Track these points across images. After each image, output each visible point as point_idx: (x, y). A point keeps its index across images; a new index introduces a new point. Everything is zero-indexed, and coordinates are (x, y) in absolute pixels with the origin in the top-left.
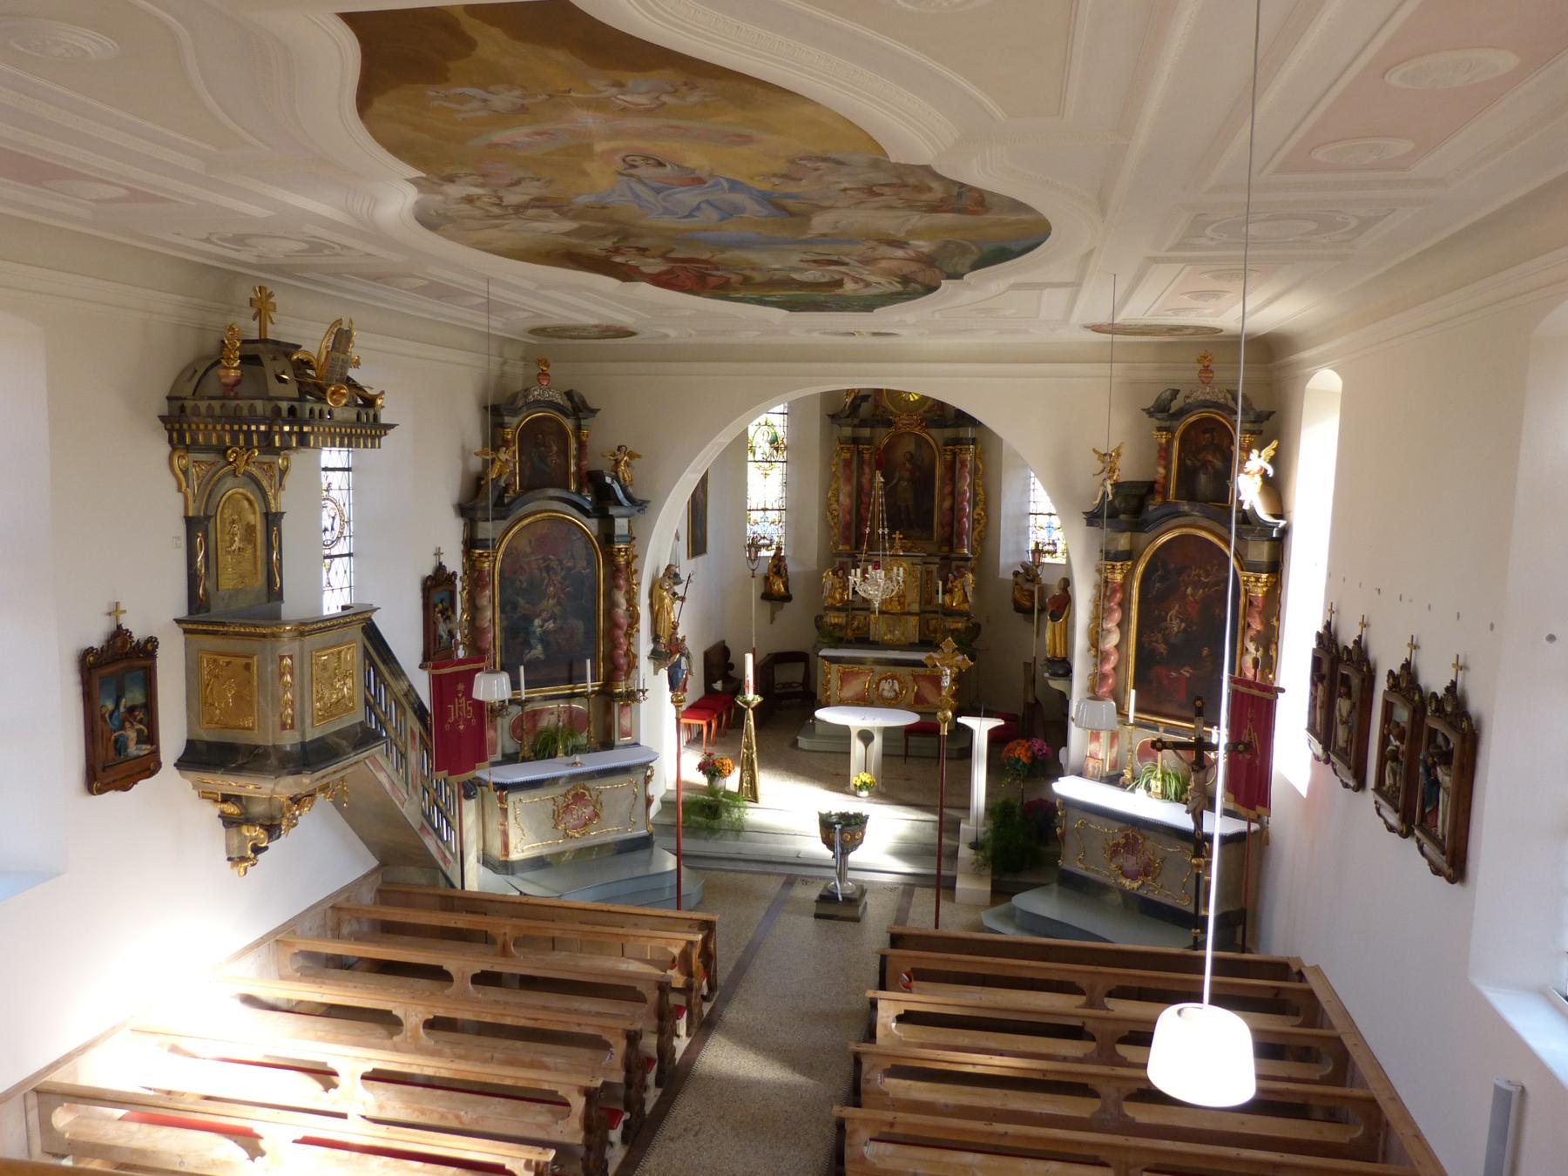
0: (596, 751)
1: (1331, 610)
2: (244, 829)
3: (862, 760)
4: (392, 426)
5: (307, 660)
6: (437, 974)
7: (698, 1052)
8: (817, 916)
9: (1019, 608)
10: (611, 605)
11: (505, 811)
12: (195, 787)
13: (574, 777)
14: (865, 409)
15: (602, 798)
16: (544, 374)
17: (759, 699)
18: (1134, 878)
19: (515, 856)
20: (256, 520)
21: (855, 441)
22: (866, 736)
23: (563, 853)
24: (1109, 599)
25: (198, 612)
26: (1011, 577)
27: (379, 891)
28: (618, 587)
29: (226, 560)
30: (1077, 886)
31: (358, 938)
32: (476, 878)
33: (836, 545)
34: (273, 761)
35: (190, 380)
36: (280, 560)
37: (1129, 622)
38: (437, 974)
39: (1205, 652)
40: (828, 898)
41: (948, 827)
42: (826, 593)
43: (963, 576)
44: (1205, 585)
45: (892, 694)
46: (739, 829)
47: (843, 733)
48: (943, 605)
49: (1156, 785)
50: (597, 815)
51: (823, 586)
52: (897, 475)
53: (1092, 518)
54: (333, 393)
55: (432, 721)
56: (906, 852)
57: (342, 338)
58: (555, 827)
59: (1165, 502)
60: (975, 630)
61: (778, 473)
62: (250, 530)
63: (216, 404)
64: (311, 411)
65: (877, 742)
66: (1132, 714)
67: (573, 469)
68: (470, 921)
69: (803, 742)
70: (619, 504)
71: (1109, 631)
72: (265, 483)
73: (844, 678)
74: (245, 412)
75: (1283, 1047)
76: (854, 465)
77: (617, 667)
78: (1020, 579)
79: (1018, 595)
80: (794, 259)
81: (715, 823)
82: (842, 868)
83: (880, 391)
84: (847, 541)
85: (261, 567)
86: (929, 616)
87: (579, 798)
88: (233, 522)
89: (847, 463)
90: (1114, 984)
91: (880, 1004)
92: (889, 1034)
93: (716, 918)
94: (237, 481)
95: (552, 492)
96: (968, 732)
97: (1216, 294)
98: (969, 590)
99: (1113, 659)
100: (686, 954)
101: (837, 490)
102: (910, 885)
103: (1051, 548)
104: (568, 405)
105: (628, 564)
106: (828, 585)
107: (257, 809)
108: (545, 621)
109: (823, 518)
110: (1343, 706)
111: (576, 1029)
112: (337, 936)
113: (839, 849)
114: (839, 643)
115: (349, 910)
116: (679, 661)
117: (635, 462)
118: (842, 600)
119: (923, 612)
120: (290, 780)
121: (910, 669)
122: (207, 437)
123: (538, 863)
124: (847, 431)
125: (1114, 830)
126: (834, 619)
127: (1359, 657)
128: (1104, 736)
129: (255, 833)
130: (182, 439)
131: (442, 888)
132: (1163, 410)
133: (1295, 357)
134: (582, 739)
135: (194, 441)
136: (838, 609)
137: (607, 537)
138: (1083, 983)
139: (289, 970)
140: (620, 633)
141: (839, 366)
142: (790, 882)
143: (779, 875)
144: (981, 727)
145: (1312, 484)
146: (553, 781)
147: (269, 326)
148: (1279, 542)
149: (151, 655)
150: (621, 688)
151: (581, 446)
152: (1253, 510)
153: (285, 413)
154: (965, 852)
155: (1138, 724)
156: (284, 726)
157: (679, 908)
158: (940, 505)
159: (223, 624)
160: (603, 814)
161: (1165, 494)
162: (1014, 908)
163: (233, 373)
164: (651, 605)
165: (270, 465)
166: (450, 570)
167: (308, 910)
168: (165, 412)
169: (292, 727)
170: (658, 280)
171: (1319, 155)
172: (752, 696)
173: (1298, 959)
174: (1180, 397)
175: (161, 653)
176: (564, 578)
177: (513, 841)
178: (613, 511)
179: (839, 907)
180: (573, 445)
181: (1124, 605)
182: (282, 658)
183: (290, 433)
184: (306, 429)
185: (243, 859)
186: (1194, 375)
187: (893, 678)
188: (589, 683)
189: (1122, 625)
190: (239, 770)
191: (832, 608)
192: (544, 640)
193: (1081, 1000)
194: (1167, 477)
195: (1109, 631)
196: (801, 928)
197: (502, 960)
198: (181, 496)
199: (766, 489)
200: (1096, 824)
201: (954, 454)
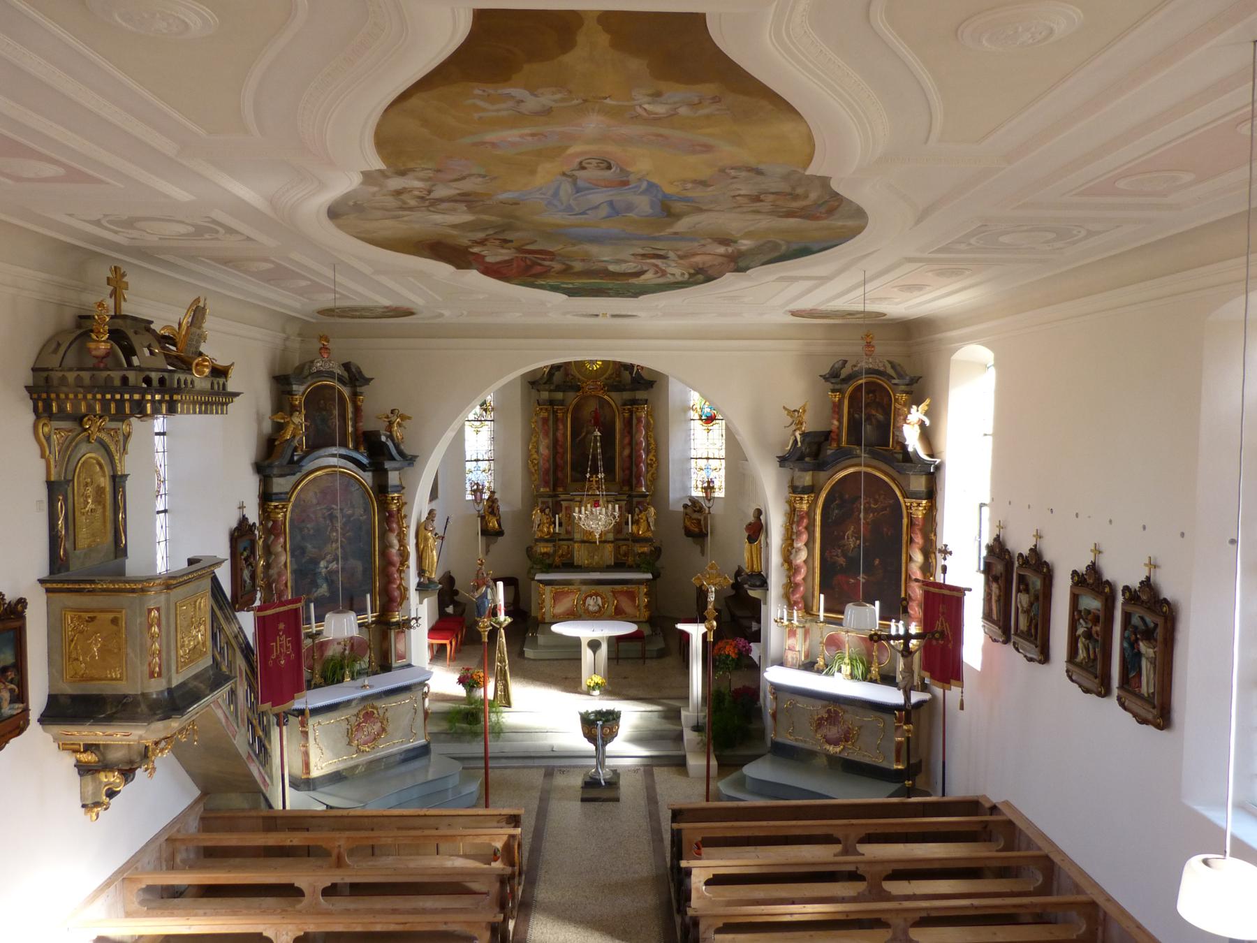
0: (375, 673)
1: (1000, 527)
2: (103, 777)
3: (592, 665)
4: (237, 394)
5: (172, 611)
6: (289, 892)
7: (526, 932)
8: (583, 800)
9: (688, 533)
10: (385, 547)
11: (305, 734)
12: (55, 740)
13: (364, 698)
14: (558, 376)
15: (388, 714)
16: (325, 348)
17: (509, 620)
18: (836, 743)
19: (315, 773)
20: (105, 482)
21: (552, 402)
22: (595, 645)
23: (356, 766)
24: (799, 524)
25: (59, 572)
27: (202, 819)
28: (391, 530)
29: (82, 520)
30: (784, 752)
31: (191, 866)
32: (295, 801)
33: (537, 488)
34: (143, 708)
35: (55, 351)
36: (125, 519)
37: (814, 542)
38: (289, 892)
39: (877, 562)
40: (591, 784)
41: (673, 715)
42: (535, 528)
43: (646, 509)
44: (874, 511)
45: (596, 608)
46: (499, 731)
47: (575, 643)
48: (632, 534)
49: (846, 669)
50: (384, 730)
51: (533, 522)
53: (783, 461)
54: (197, 365)
55: (257, 657)
56: (640, 739)
57: (198, 313)
58: (349, 744)
59: (839, 447)
60: (657, 552)
61: (486, 430)
62: (100, 491)
63: (86, 375)
64: (179, 381)
65: (604, 648)
66: (822, 614)
67: (350, 429)
68: (297, 838)
69: (529, 653)
70: (393, 459)
71: (799, 549)
72: (113, 448)
73: (557, 597)
74: (117, 382)
75: (1006, 868)
76: (551, 422)
77: (390, 600)
78: (689, 511)
79: (688, 524)
80: (626, 253)
81: (479, 728)
82: (600, 756)
83: (570, 363)
84: (546, 484)
85: (110, 526)
86: (621, 543)
87: (368, 716)
88: (87, 485)
89: (545, 421)
90: (863, 832)
91: (694, 872)
92: (701, 897)
93: (521, 812)
94: (90, 446)
95: (334, 450)
96: (685, 637)
97: (919, 288)
98: (651, 520)
99: (803, 571)
100: (508, 847)
101: (537, 442)
102: (650, 765)
104: (346, 374)
105: (399, 510)
106: (537, 522)
107: (114, 756)
108: (329, 562)
110: (1020, 600)
111: (443, 928)
112: (172, 867)
113: (600, 742)
114: (550, 568)
115: (183, 840)
116: (486, 592)
117: (406, 423)
118: (549, 533)
119: (616, 540)
120: (159, 725)
121: (609, 587)
122: (76, 406)
123: (336, 778)
124: (545, 395)
125: (819, 709)
126: (543, 548)
127: (1037, 564)
128: (800, 632)
129: (113, 778)
130: (48, 407)
131: (264, 812)
132: (836, 377)
133: (939, 336)
134: (363, 664)
135: (61, 409)
136: (547, 541)
137: (382, 489)
138: (838, 834)
139: (135, 905)
140: (394, 569)
141: (585, 342)
142: (549, 773)
143: (538, 767)
144: (696, 632)
145: (966, 434)
146: (348, 703)
147: (123, 304)
148: (933, 476)
149: (21, 617)
150: (397, 618)
151: (357, 410)
152: (916, 452)
153: (155, 383)
154: (689, 735)
155: (828, 621)
156: (152, 675)
157: (487, 807)
158: (621, 452)
159: (92, 582)
160: (390, 728)
161: (839, 441)
162: (744, 776)
163: (102, 346)
164: (417, 545)
165: (116, 430)
166: (251, 521)
167: (147, 845)
168: (30, 383)
169: (160, 675)
170: (493, 271)
171: (1121, 184)
172: (502, 617)
173: (984, 796)
174: (848, 366)
175: (29, 613)
176: (345, 524)
177: (313, 760)
178: (387, 465)
179: (600, 790)
180: (350, 409)
181: (810, 529)
182: (150, 611)
183: (160, 402)
184: (175, 397)
185: (97, 804)
186: (859, 348)
187: (597, 595)
188: (370, 615)
189: (809, 544)
190: (110, 719)
191: (541, 540)
192: (330, 579)
193: (838, 848)
194: (840, 428)
195: (799, 549)
196: (568, 812)
197: (338, 872)
198: (43, 462)
199: (479, 441)
200: (802, 703)
201: (631, 412)
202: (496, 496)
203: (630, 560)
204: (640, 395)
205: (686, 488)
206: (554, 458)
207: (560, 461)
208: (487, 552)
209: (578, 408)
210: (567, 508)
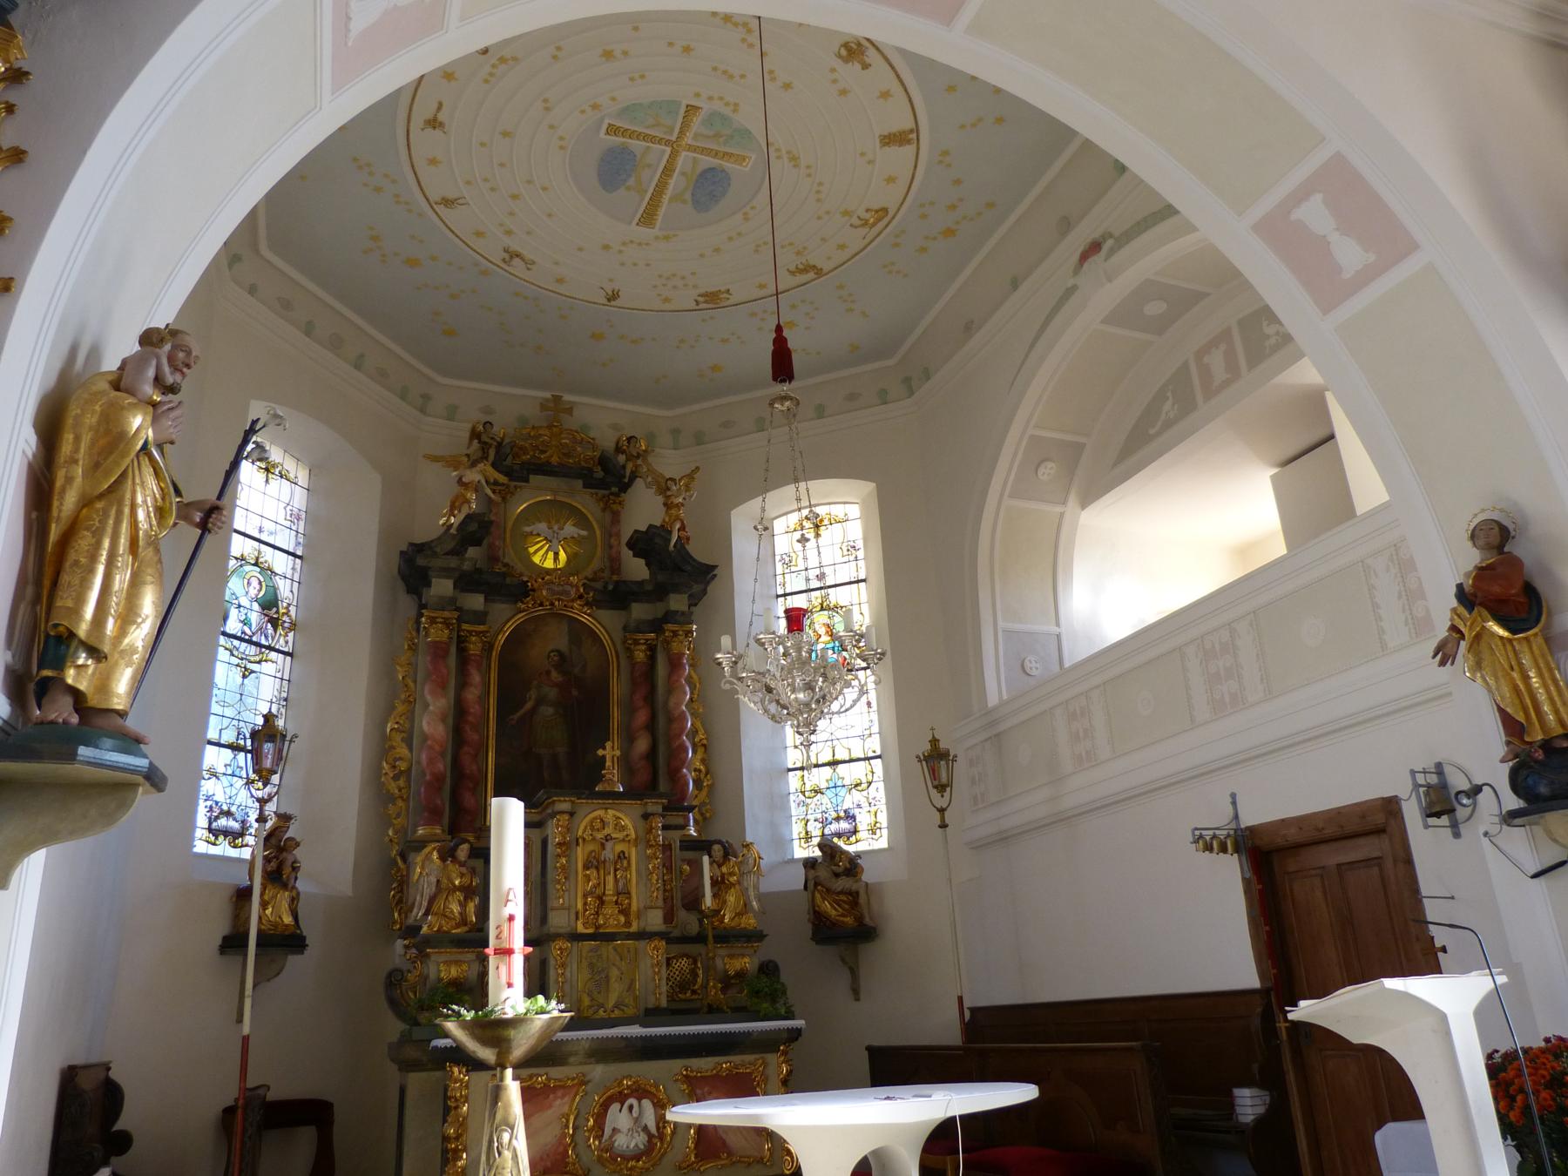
45: (640, 1140)
52: (533, 694)
76: (452, 660)
78: (823, 873)
79: (827, 907)
84: (434, 815)
89: (438, 651)
101: (410, 716)
103: (844, 825)
109: (374, 779)
118: (464, 921)
121: (676, 1065)
187: (640, 1092)
203: (714, 992)
204: (677, 602)
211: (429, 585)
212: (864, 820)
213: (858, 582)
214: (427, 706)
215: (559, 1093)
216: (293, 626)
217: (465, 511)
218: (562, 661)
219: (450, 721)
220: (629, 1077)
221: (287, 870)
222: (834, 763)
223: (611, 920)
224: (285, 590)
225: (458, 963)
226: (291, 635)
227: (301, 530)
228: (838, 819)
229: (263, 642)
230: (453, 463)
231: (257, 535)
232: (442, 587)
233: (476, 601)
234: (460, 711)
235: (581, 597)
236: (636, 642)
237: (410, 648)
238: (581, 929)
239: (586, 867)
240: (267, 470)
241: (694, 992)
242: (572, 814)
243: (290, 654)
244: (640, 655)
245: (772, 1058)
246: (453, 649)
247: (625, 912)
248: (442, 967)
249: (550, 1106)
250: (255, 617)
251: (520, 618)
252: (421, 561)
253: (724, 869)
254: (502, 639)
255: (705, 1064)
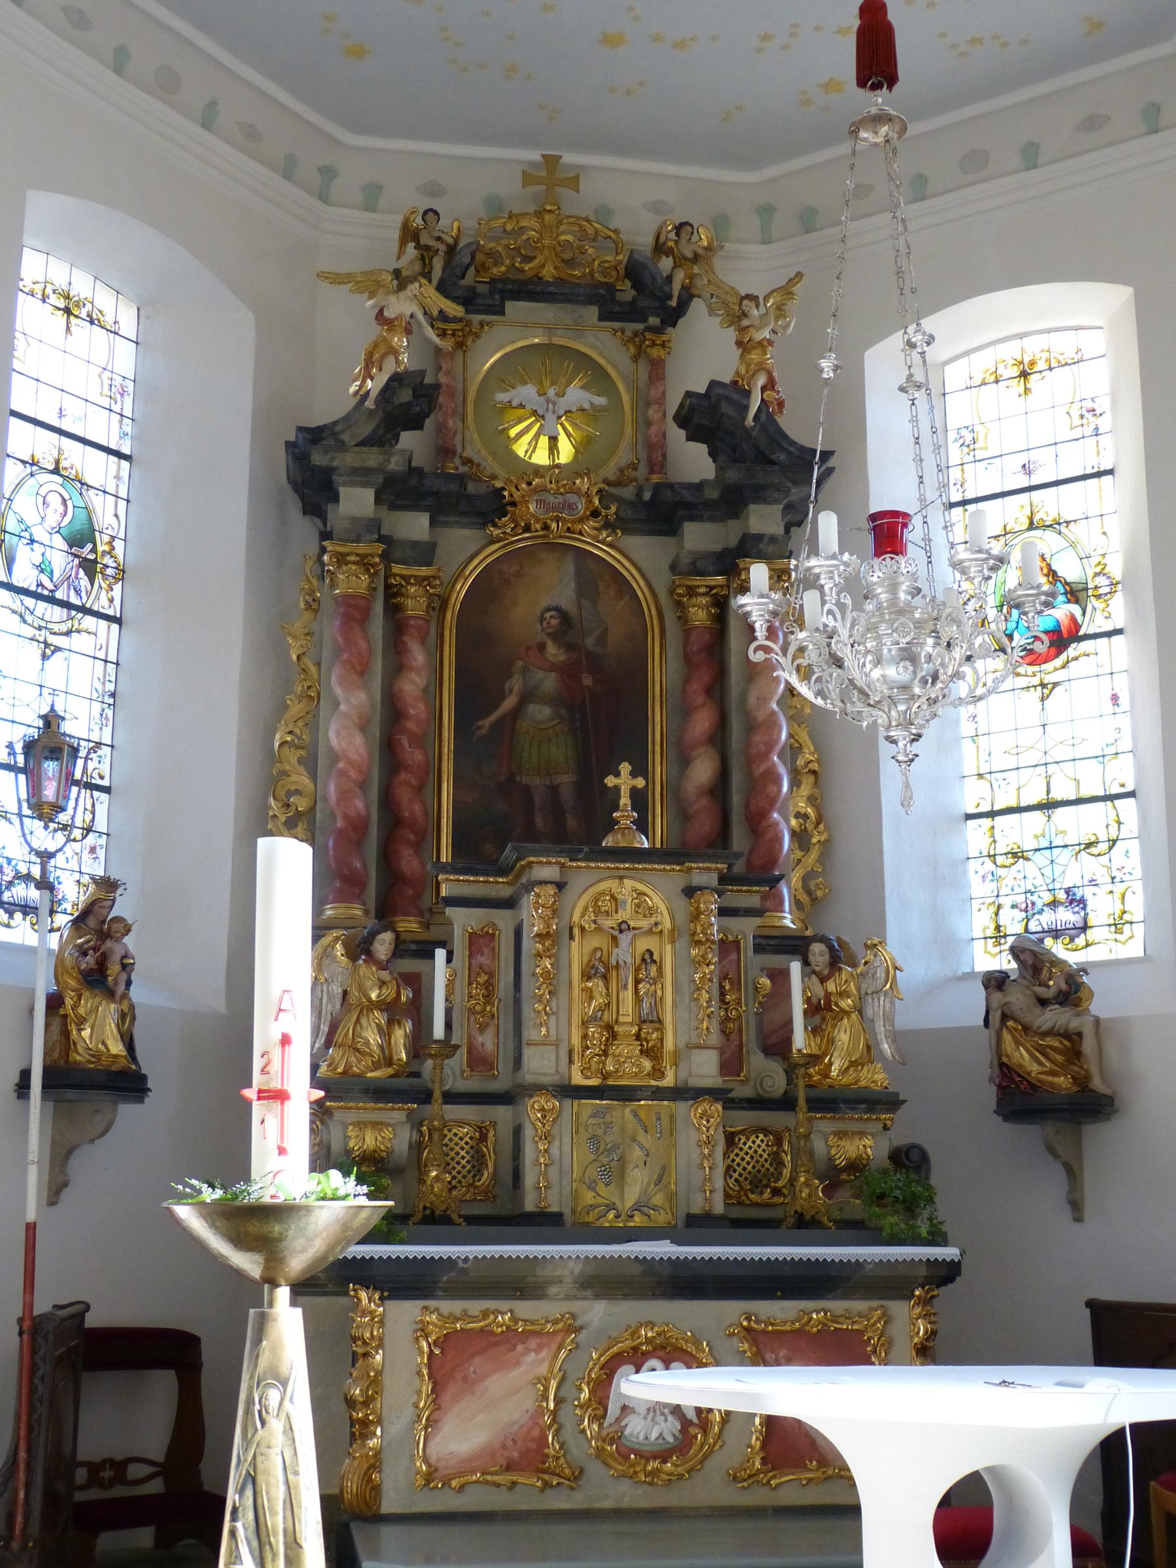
9: (1017, 1098)
26: (971, 1007)
52: (516, 684)
76: (377, 626)
78: (1017, 998)
79: (1023, 1057)
89: (354, 612)
101: (312, 721)
103: (1066, 916)
121: (733, 1310)
136: (380, 1093)
172: (283, 1159)
201: (721, 605)
202: (123, 907)
203: (809, 1193)
204: (764, 519)
205: (948, 943)
206: (387, 800)
207: (411, 807)
208: (56, 1189)
209: (489, 589)
210: (480, 941)
211: (335, 498)
212: (1100, 908)
213: (1099, 474)
214: (336, 704)
215: (533, 1343)
216: (121, 573)
217: (390, 368)
218: (565, 626)
219: (376, 730)
220: (651, 1324)
221: (114, 969)
222: (1048, 806)
223: (629, 1064)
224: (108, 516)
225: (377, 1125)
226: (117, 588)
227: (128, 412)
228: (1054, 904)
229: (74, 600)
230: (368, 284)
231: (55, 422)
232: (356, 501)
233: (415, 525)
234: (393, 711)
235: (595, 514)
236: (692, 592)
237: (308, 606)
238: (578, 1079)
239: (586, 976)
240: (68, 311)
241: (776, 1192)
242: (560, 886)
243: (117, 620)
244: (699, 614)
245: (901, 1310)
246: (378, 608)
247: (653, 1052)
248: (352, 1132)
249: (518, 1363)
250: (60, 561)
251: (492, 552)
252: (318, 458)
253: (831, 986)
254: (461, 589)
255: (780, 1312)
